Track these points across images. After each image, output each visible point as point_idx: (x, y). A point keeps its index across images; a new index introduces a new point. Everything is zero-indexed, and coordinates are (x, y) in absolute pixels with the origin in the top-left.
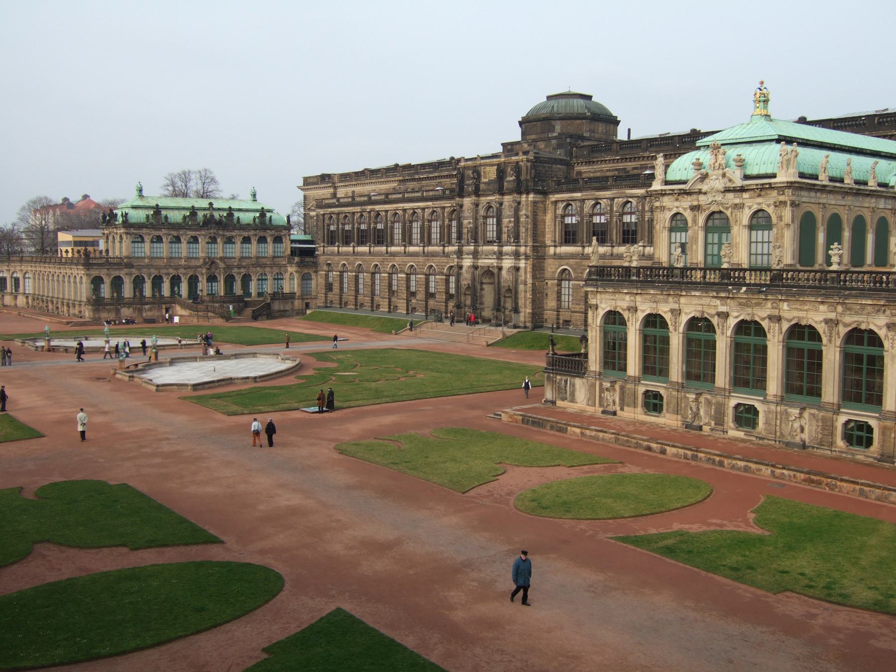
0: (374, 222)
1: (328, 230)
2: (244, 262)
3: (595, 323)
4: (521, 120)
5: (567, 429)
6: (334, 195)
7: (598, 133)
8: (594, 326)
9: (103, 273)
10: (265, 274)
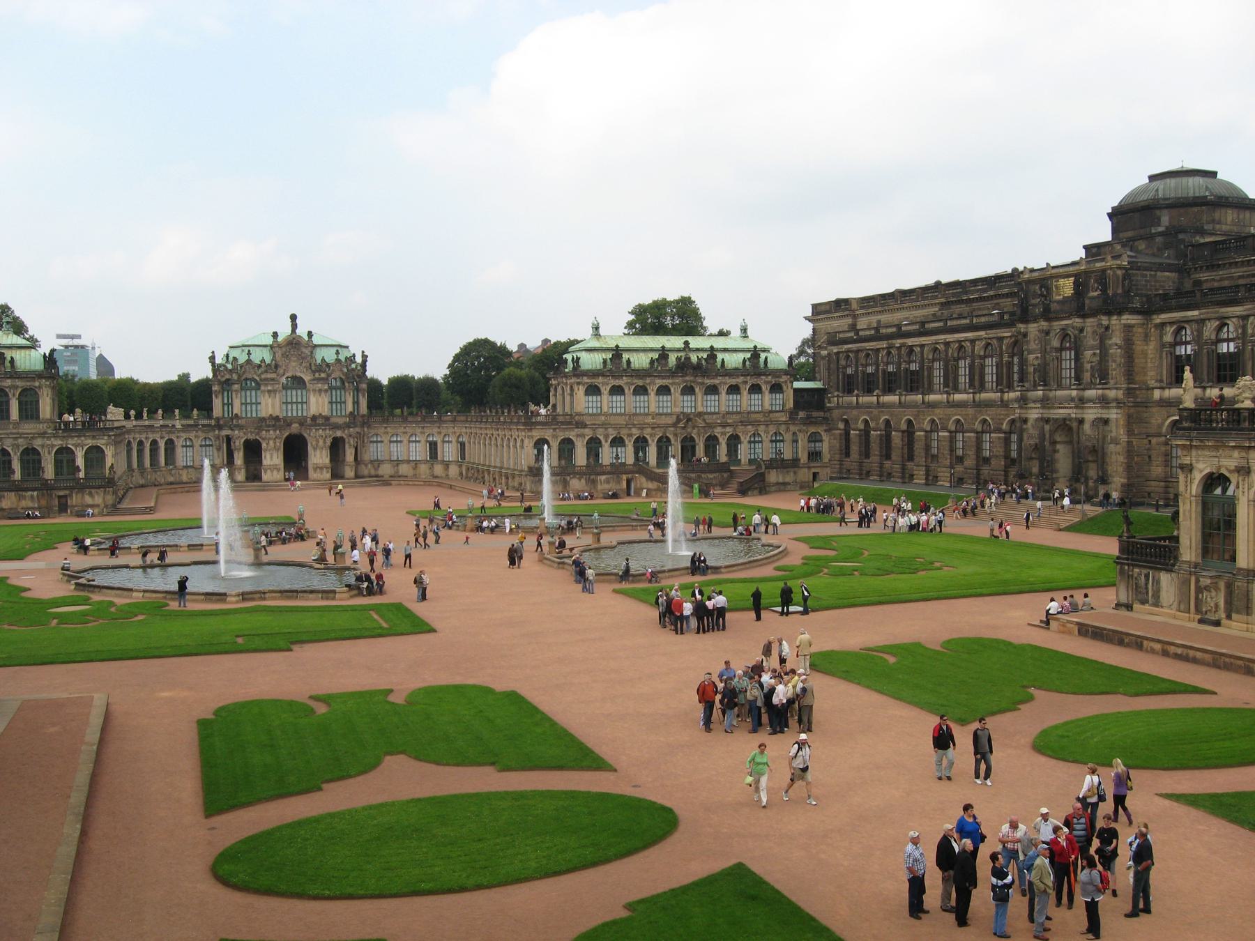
0: (905, 361)
1: (844, 374)
2: (730, 419)
3: (1189, 491)
4: (1110, 211)
5: (1142, 643)
6: (853, 327)
7: (1226, 224)
8: (1188, 495)
9: (547, 434)
10: (758, 434)
